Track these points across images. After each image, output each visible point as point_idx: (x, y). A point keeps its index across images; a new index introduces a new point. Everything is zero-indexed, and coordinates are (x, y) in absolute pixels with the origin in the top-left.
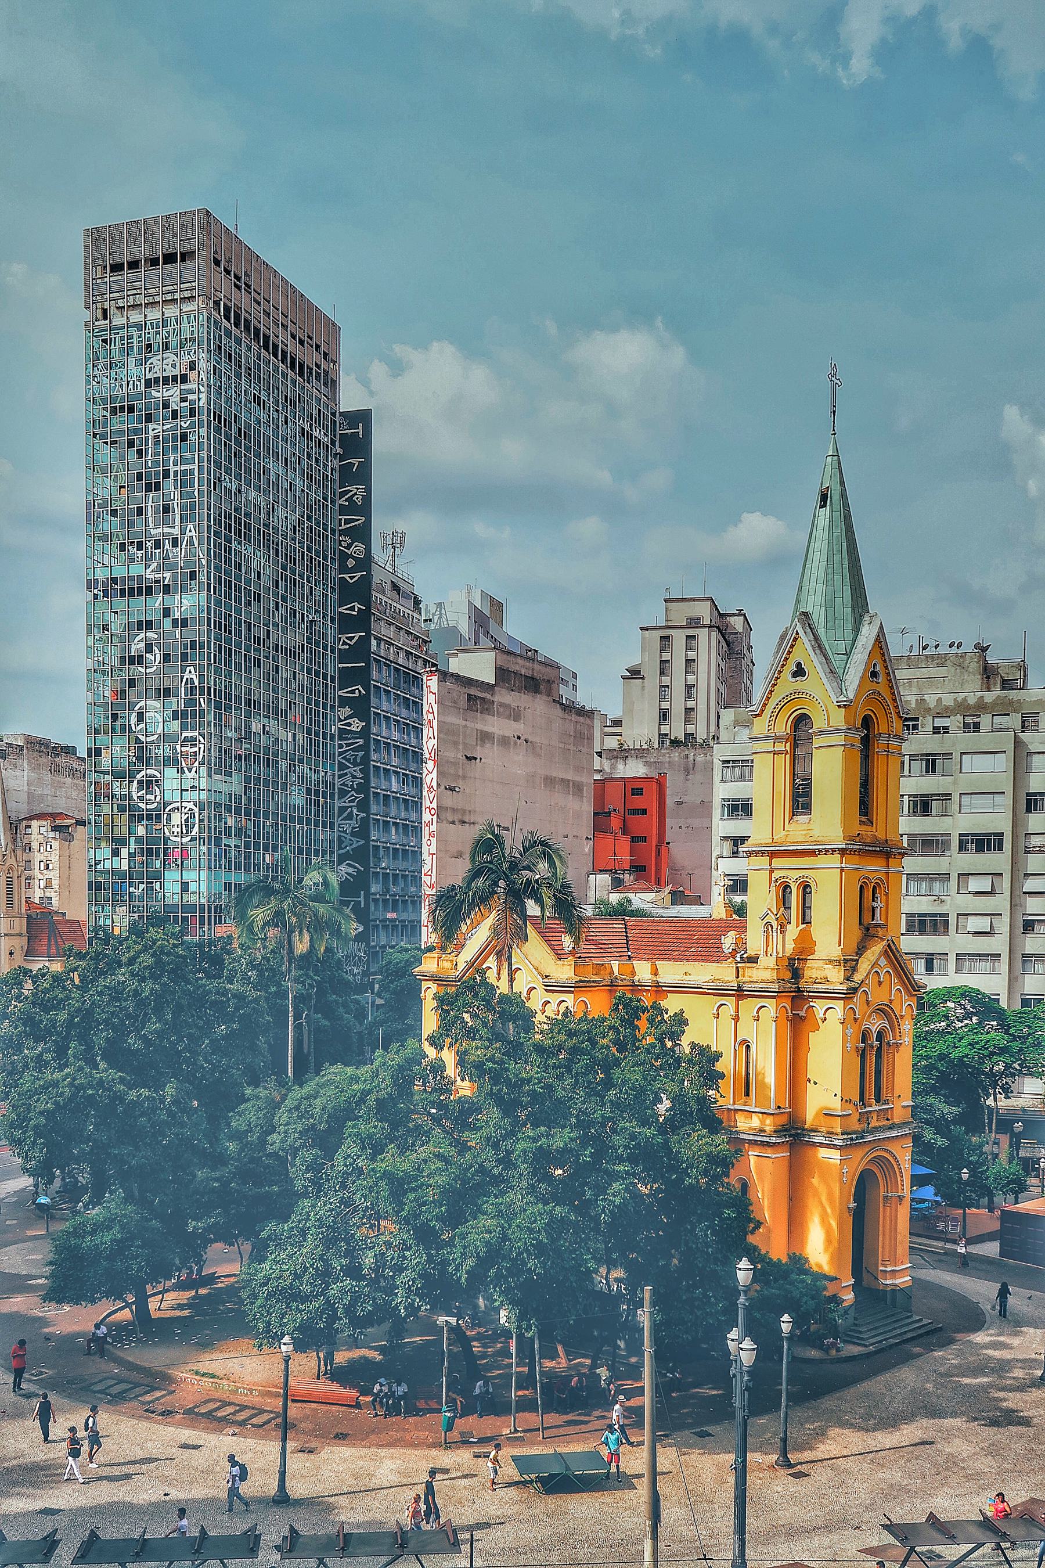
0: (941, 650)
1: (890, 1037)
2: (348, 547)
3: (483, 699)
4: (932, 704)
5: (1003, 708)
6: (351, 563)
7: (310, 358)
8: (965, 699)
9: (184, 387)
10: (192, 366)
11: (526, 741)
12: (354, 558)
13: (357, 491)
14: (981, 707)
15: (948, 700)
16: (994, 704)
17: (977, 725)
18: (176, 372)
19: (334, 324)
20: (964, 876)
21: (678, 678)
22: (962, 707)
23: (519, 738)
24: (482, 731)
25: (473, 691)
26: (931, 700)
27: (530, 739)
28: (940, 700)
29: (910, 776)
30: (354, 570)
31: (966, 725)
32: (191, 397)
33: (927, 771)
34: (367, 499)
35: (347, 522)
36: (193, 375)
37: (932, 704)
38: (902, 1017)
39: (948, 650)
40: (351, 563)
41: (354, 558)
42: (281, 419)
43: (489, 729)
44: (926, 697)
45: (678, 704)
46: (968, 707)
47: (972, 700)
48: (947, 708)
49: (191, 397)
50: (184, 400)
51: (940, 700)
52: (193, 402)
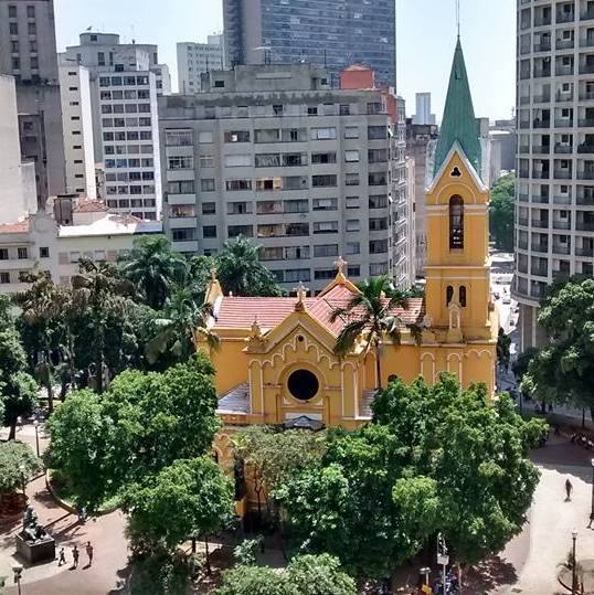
4: (290, 97)
5: (329, 100)
8: (308, 95)
14: (317, 100)
15: (298, 95)
17: (315, 111)
20: (316, 201)
21: (24, 36)
22: (306, 99)
26: (289, 94)
28: (294, 95)
31: (310, 111)
37: (290, 97)
44: (286, 93)
45: (25, 56)
51: (294, 95)
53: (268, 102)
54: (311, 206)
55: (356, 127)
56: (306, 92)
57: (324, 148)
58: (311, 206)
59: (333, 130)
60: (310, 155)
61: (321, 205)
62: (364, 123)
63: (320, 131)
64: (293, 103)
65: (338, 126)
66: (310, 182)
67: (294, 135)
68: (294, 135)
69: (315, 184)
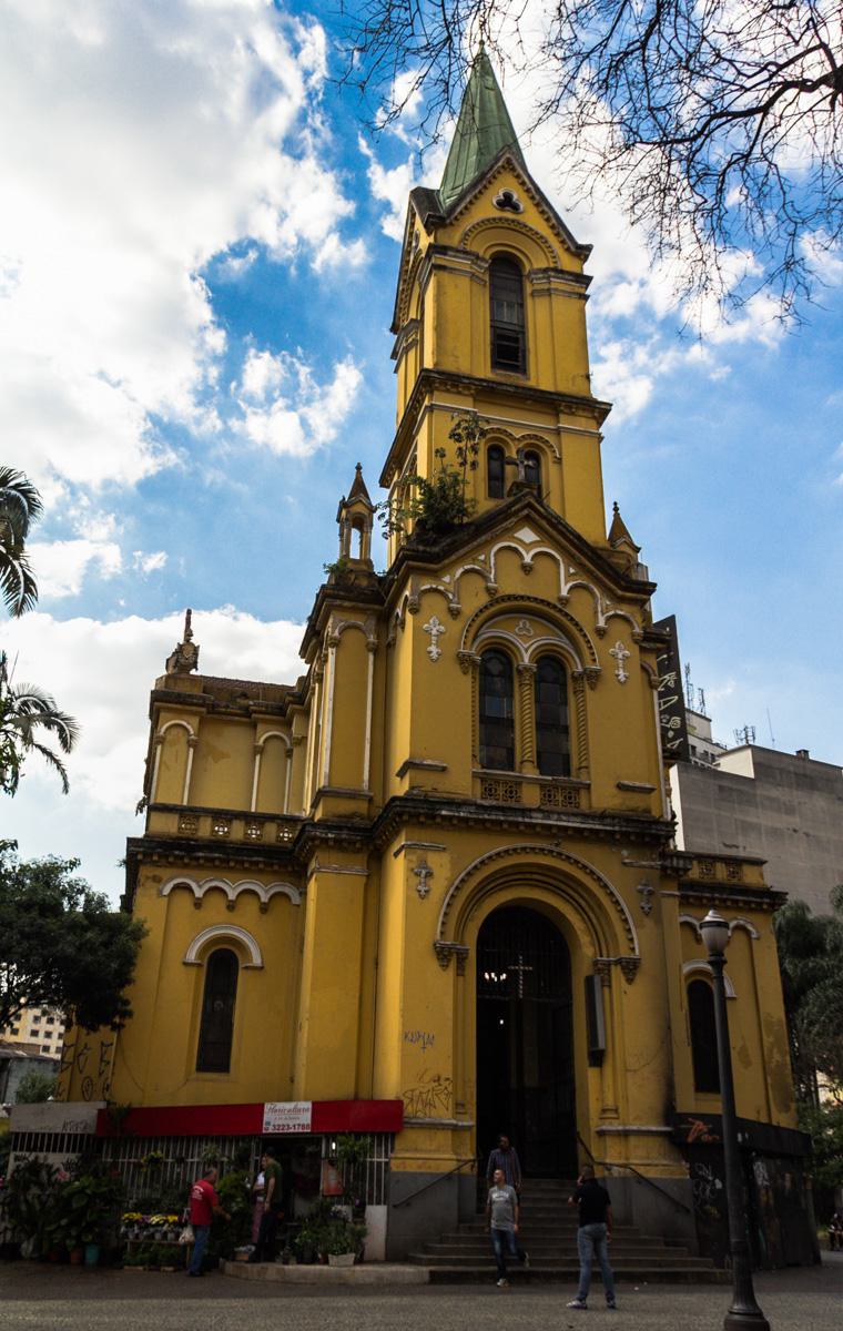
2: (667, 723)
3: (741, 792)
6: (671, 734)
11: (807, 835)
12: (673, 730)
13: (669, 678)
23: (795, 831)
24: (743, 822)
25: (725, 783)
27: (811, 832)
30: (674, 738)
34: (678, 682)
35: (665, 703)
40: (671, 734)
41: (673, 730)
43: (749, 819)
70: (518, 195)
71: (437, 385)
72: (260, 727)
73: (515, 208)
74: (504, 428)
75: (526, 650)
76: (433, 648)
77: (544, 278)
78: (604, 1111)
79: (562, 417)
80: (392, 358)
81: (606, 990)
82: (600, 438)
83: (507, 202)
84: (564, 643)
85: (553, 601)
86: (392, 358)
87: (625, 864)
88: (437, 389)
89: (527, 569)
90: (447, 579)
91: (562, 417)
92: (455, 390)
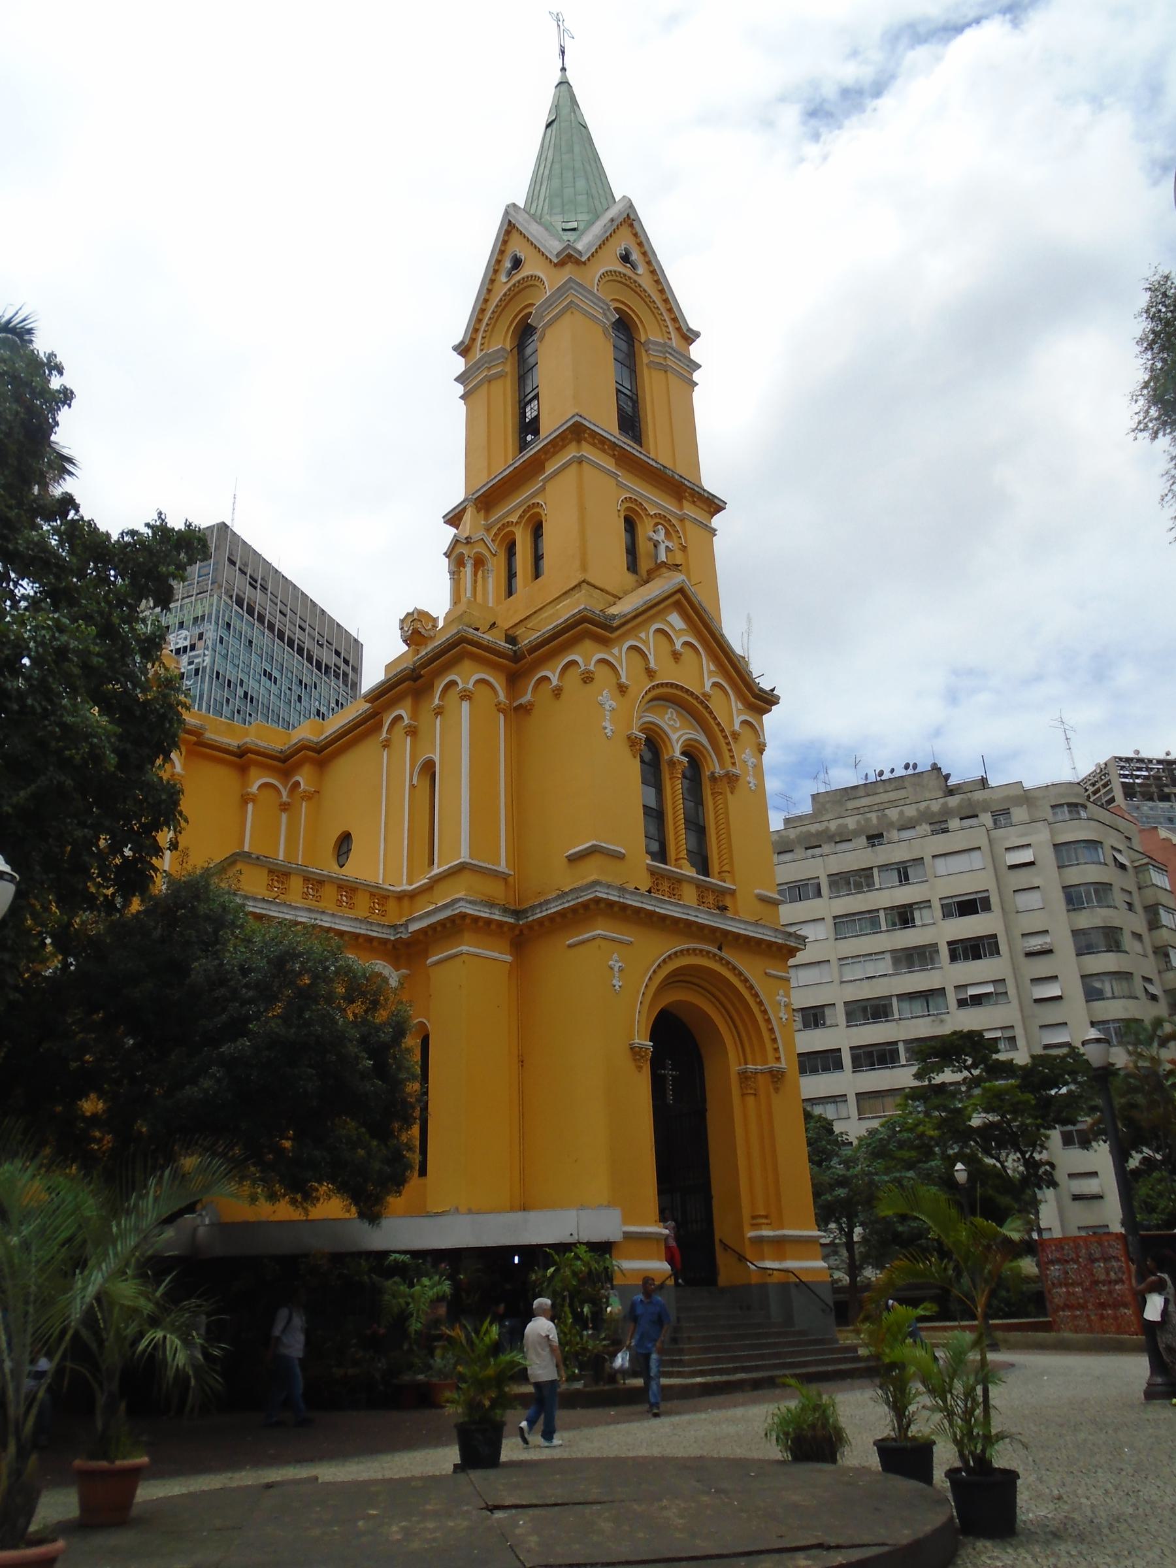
0: (897, 774)
1: (712, 766)
7: (328, 658)
8: (928, 808)
9: (193, 653)
10: (201, 636)
15: (911, 812)
16: (960, 806)
18: (187, 643)
19: (356, 641)
28: (901, 813)
29: (881, 889)
32: (196, 661)
33: (901, 881)
36: (200, 644)
38: (735, 735)
39: (903, 772)
42: (294, 697)
46: (933, 814)
47: (935, 807)
48: (911, 819)
49: (196, 661)
50: (190, 663)
51: (901, 813)
52: (199, 663)
53: (857, 833)
54: (952, 997)
55: (1029, 845)
56: (923, 805)
57: (965, 887)
58: (952, 997)
59: (976, 855)
60: (936, 905)
61: (972, 991)
62: (1042, 837)
63: (950, 859)
64: (902, 828)
65: (983, 842)
66: (944, 951)
67: (903, 873)
68: (903, 873)
69: (954, 958)
70: (635, 256)
71: (586, 435)
72: (253, 772)
73: (634, 267)
74: (640, 500)
75: (677, 742)
76: (607, 724)
77: (661, 352)
78: (754, 1217)
79: (685, 503)
80: (457, 379)
81: (751, 1100)
82: (713, 532)
83: (626, 258)
84: (703, 740)
85: (697, 692)
86: (457, 379)
87: (766, 973)
88: (585, 440)
89: (676, 656)
90: (615, 651)
91: (685, 503)
92: (600, 446)
